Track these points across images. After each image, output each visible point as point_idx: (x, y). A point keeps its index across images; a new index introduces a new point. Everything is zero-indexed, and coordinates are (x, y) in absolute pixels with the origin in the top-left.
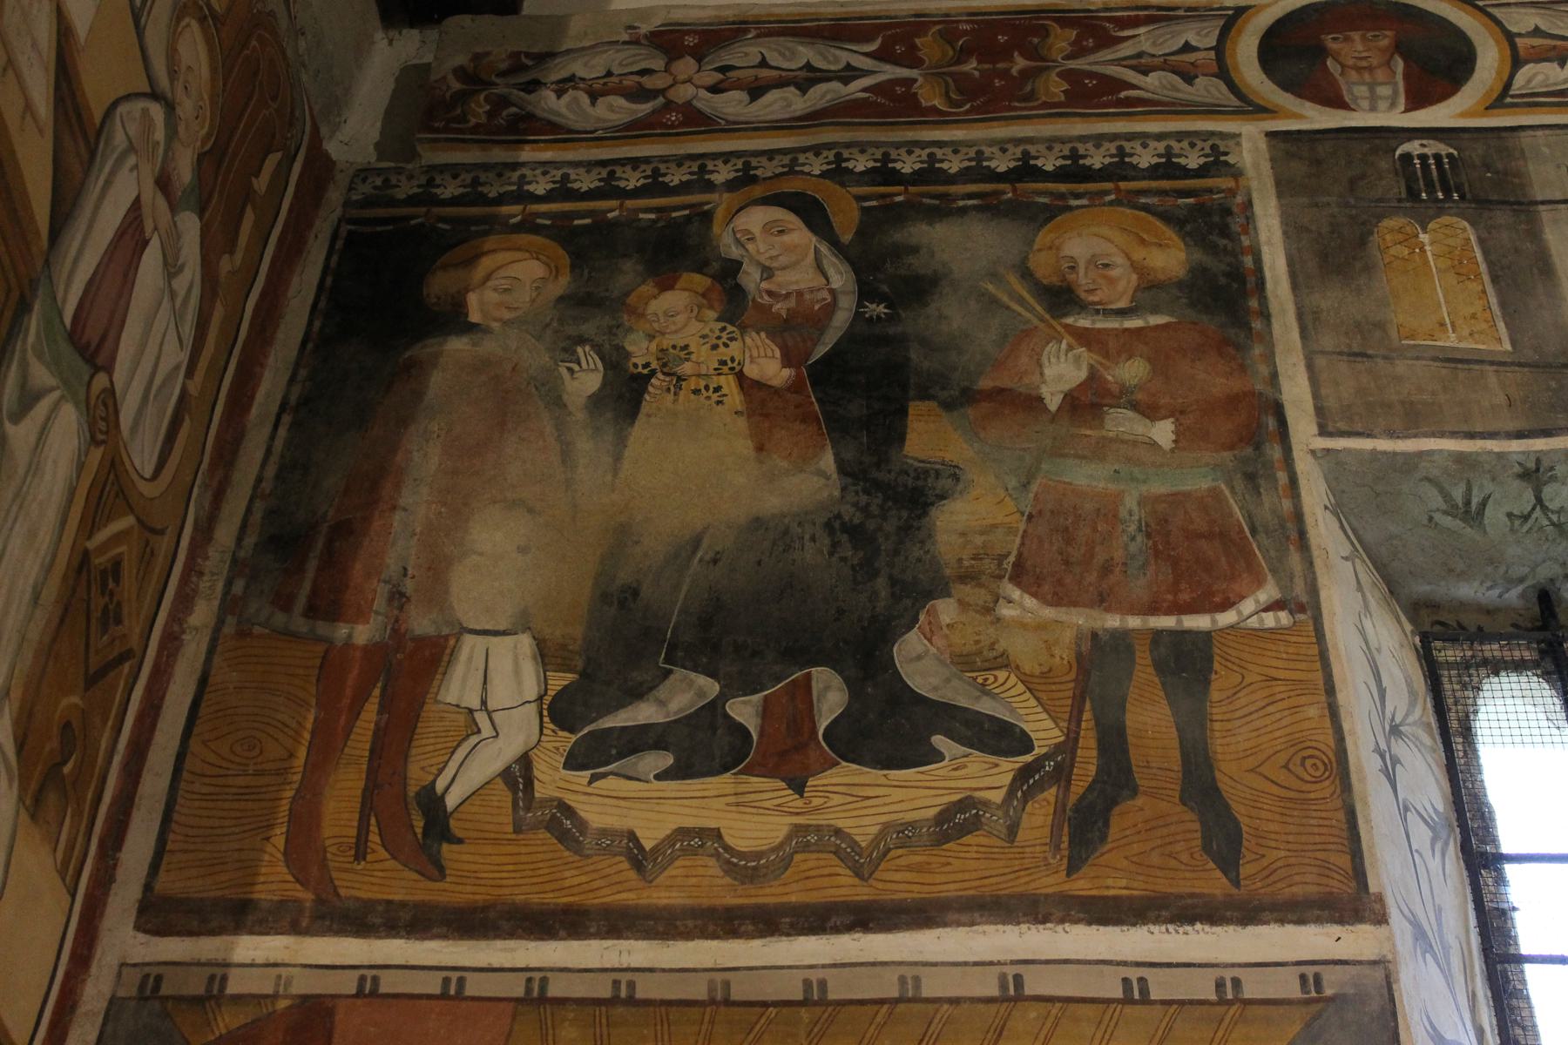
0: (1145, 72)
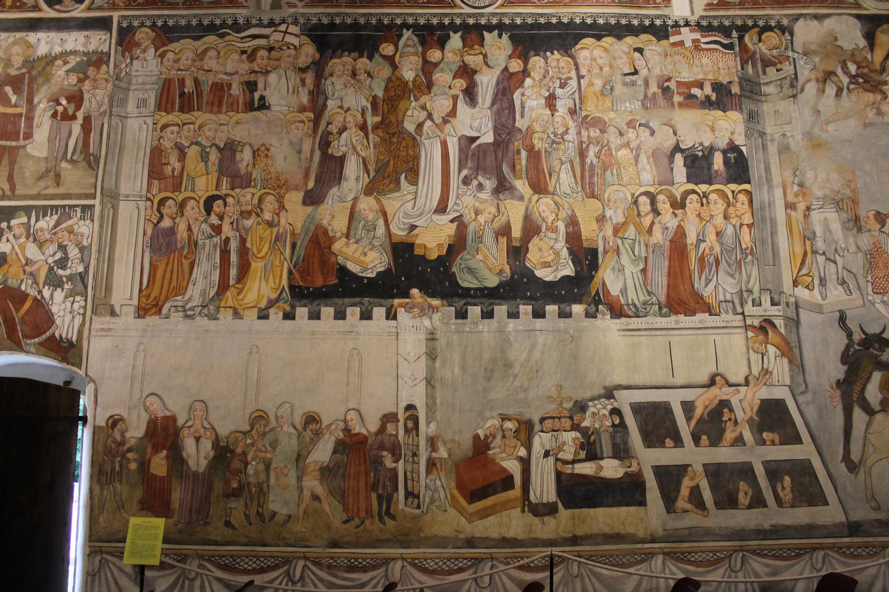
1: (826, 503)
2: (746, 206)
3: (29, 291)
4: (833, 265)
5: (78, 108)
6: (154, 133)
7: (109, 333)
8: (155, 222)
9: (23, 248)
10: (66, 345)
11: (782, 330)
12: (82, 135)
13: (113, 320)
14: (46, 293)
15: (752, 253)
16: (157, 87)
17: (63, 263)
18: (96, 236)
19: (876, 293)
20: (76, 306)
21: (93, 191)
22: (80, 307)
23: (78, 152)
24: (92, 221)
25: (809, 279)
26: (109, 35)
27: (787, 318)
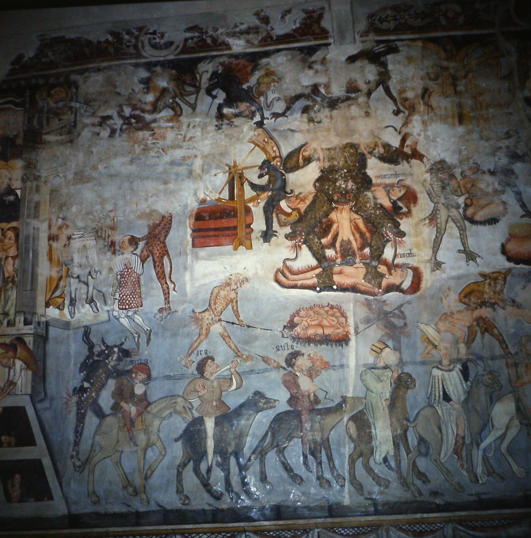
1: (51, 498)
2: (12, 241)
4: (84, 286)
11: (31, 347)
15: (13, 282)
19: (123, 309)
25: (60, 300)
27: (36, 335)
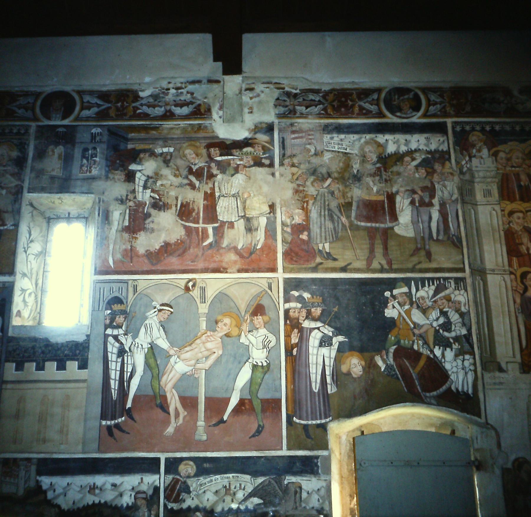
0: (19, 109)
3: (421, 350)
5: (432, 196)
6: (504, 219)
7: (501, 387)
8: (521, 292)
9: (408, 312)
10: (463, 397)
12: (441, 219)
13: (502, 375)
14: (438, 352)
16: (497, 180)
17: (447, 326)
18: (471, 303)
20: (466, 363)
21: (462, 266)
22: (471, 364)
23: (442, 233)
24: (466, 290)
26: (445, 137)
